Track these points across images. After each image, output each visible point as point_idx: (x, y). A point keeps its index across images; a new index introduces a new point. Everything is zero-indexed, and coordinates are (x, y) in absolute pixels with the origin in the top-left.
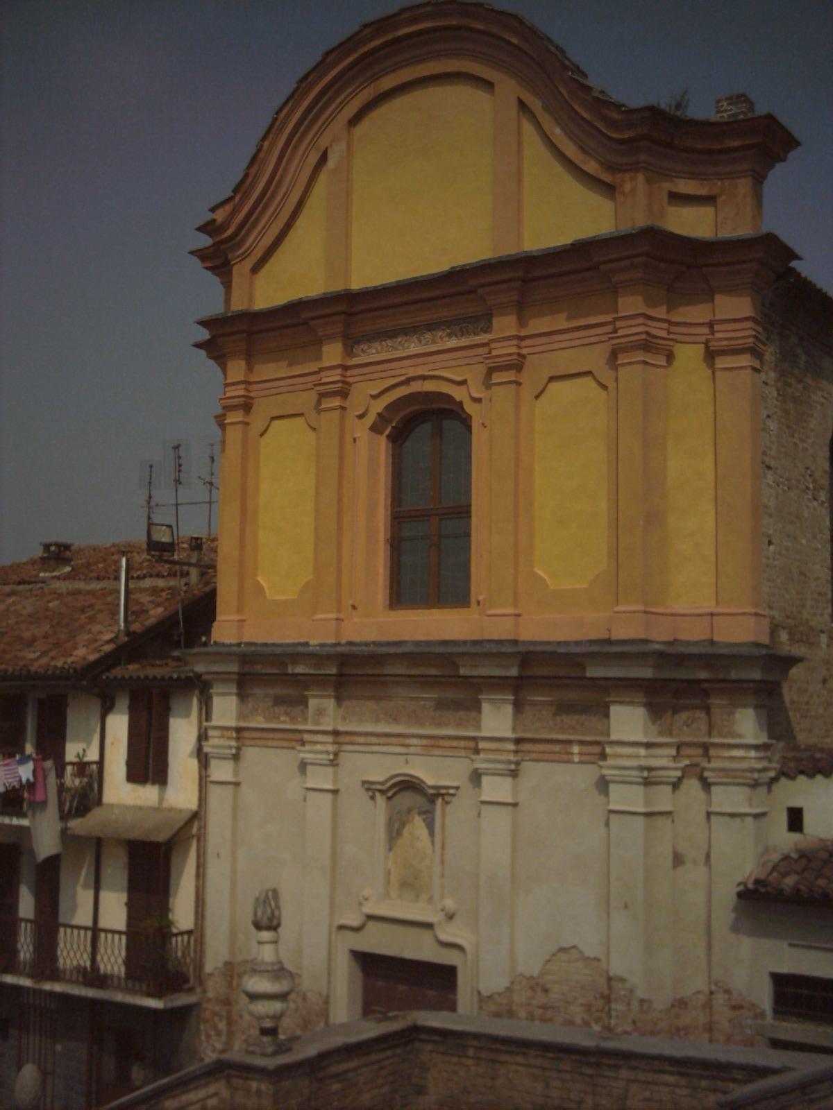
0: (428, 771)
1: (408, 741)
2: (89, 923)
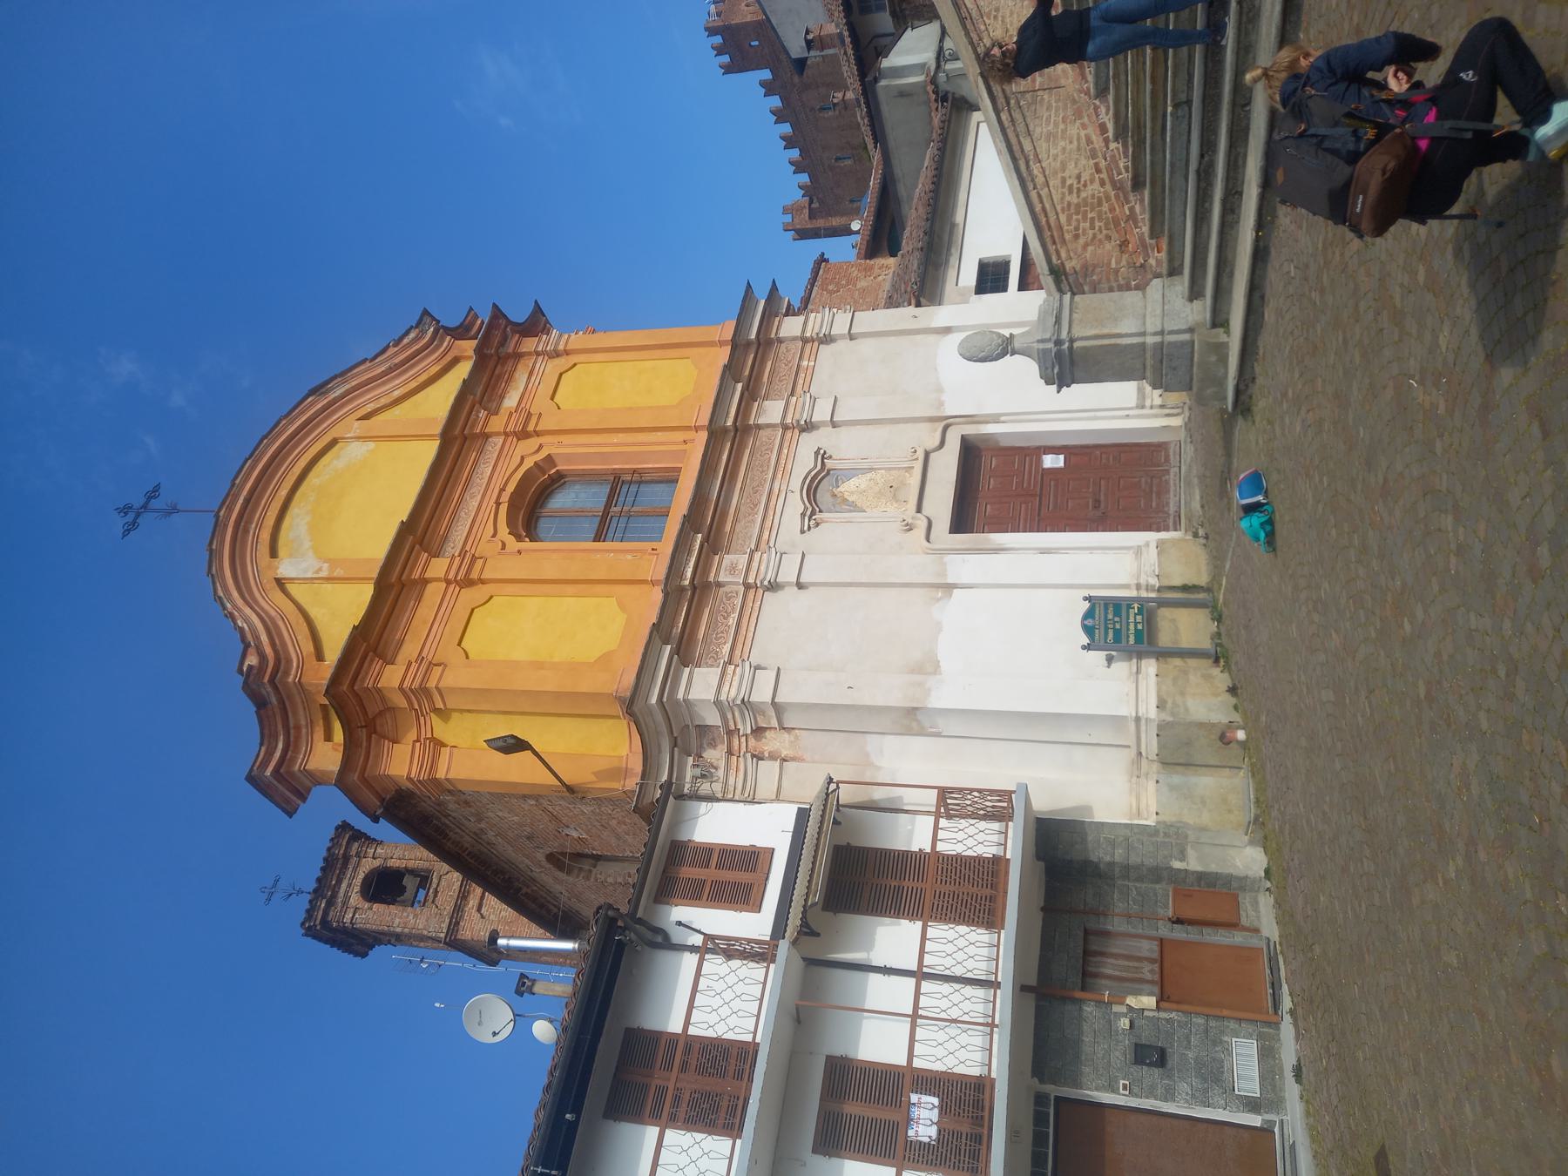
0: (803, 462)
1: (776, 491)
2: (912, 981)
